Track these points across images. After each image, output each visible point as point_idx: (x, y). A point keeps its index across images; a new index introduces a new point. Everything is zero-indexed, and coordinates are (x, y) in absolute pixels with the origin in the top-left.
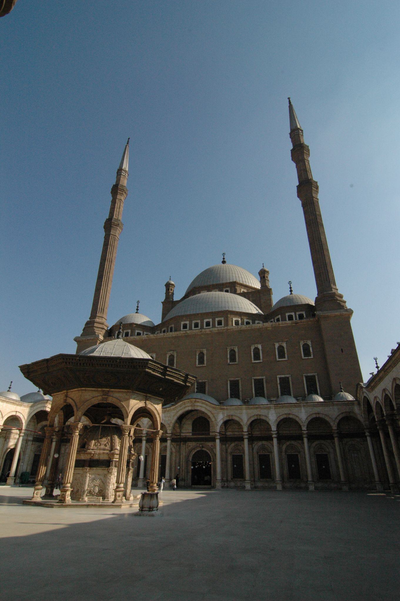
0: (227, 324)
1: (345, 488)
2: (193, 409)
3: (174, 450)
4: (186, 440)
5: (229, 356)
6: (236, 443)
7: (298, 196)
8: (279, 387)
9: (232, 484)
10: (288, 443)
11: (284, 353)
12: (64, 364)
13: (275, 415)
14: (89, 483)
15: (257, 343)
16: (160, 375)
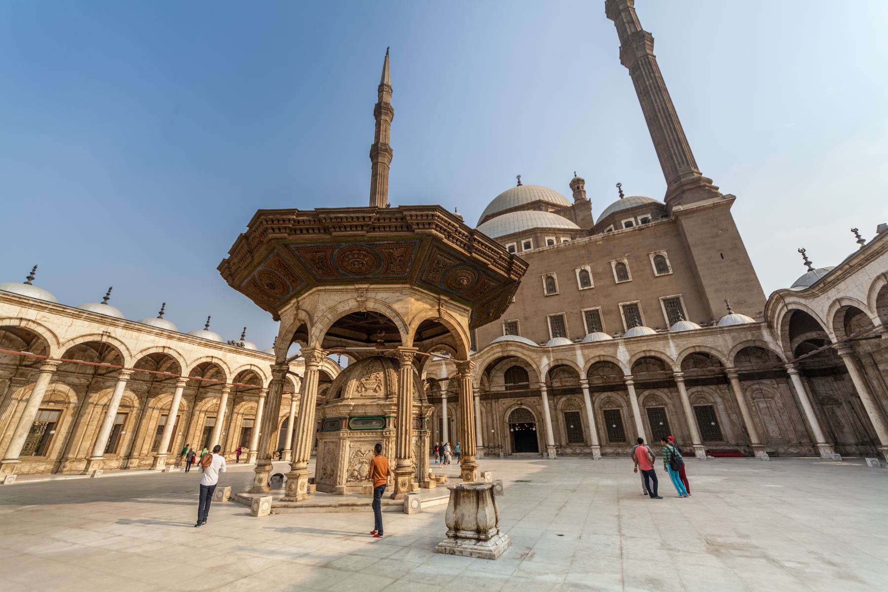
0: (537, 245)
1: (761, 454)
2: (505, 354)
3: (484, 410)
4: (497, 396)
5: (545, 286)
6: (569, 396)
7: (622, 63)
8: (624, 319)
9: (568, 451)
10: (646, 393)
11: (626, 273)
12: (271, 231)
13: (627, 353)
14: (350, 458)
15: (583, 264)
16: (463, 251)
